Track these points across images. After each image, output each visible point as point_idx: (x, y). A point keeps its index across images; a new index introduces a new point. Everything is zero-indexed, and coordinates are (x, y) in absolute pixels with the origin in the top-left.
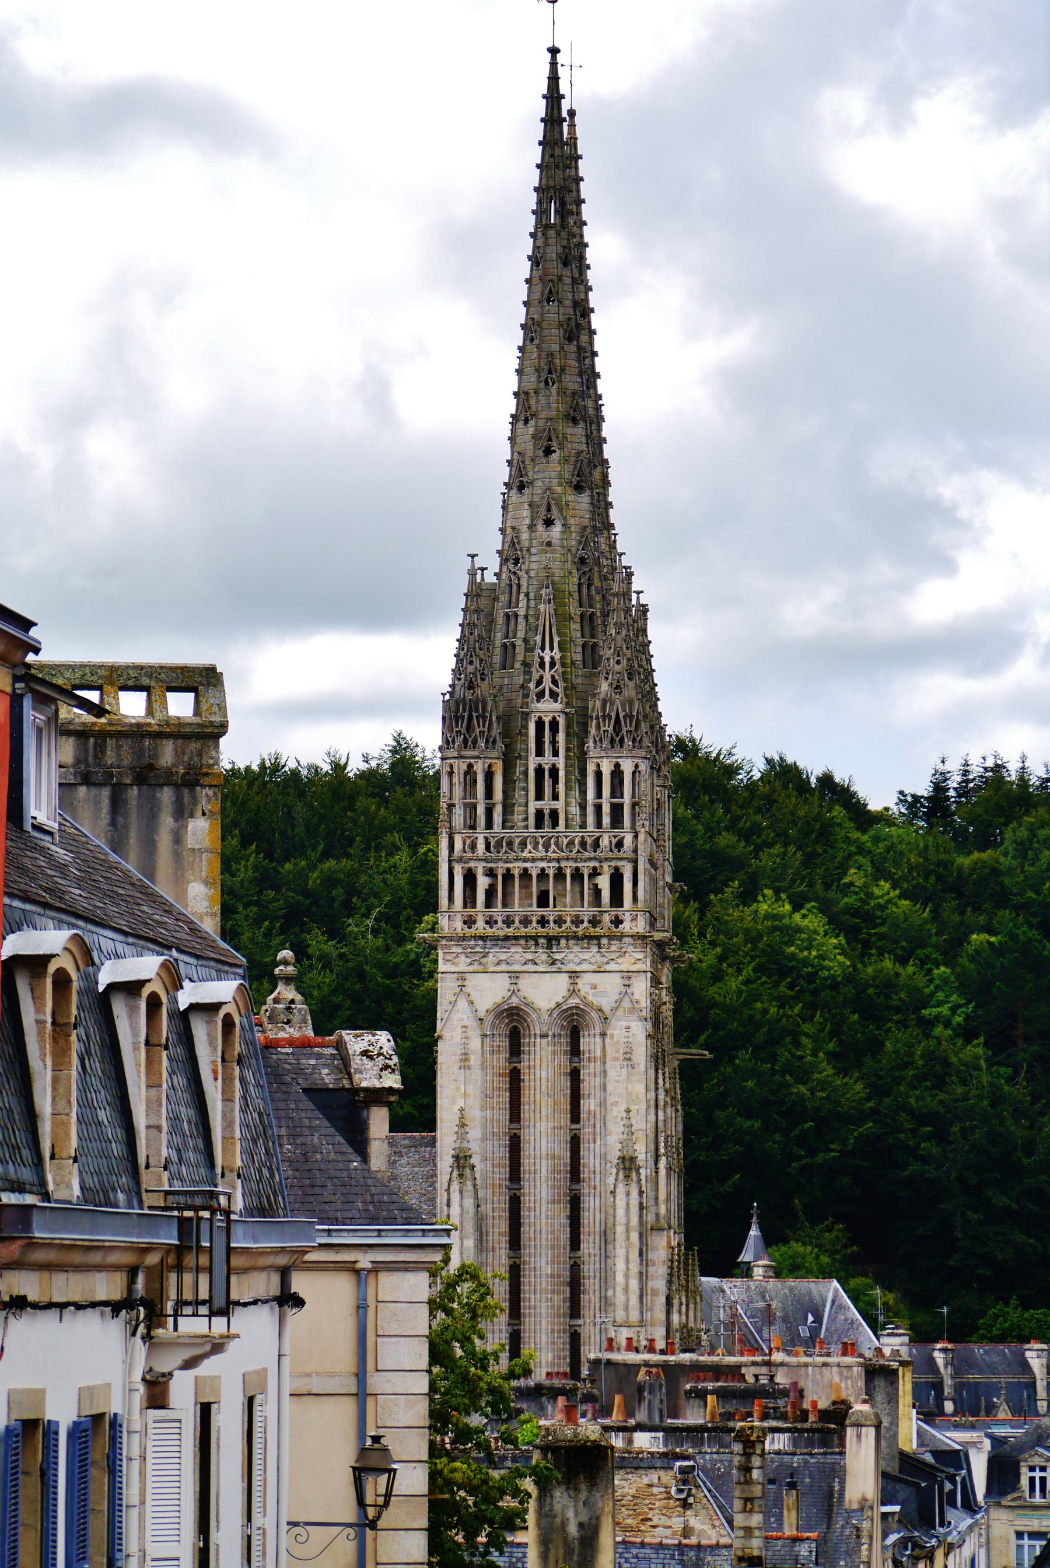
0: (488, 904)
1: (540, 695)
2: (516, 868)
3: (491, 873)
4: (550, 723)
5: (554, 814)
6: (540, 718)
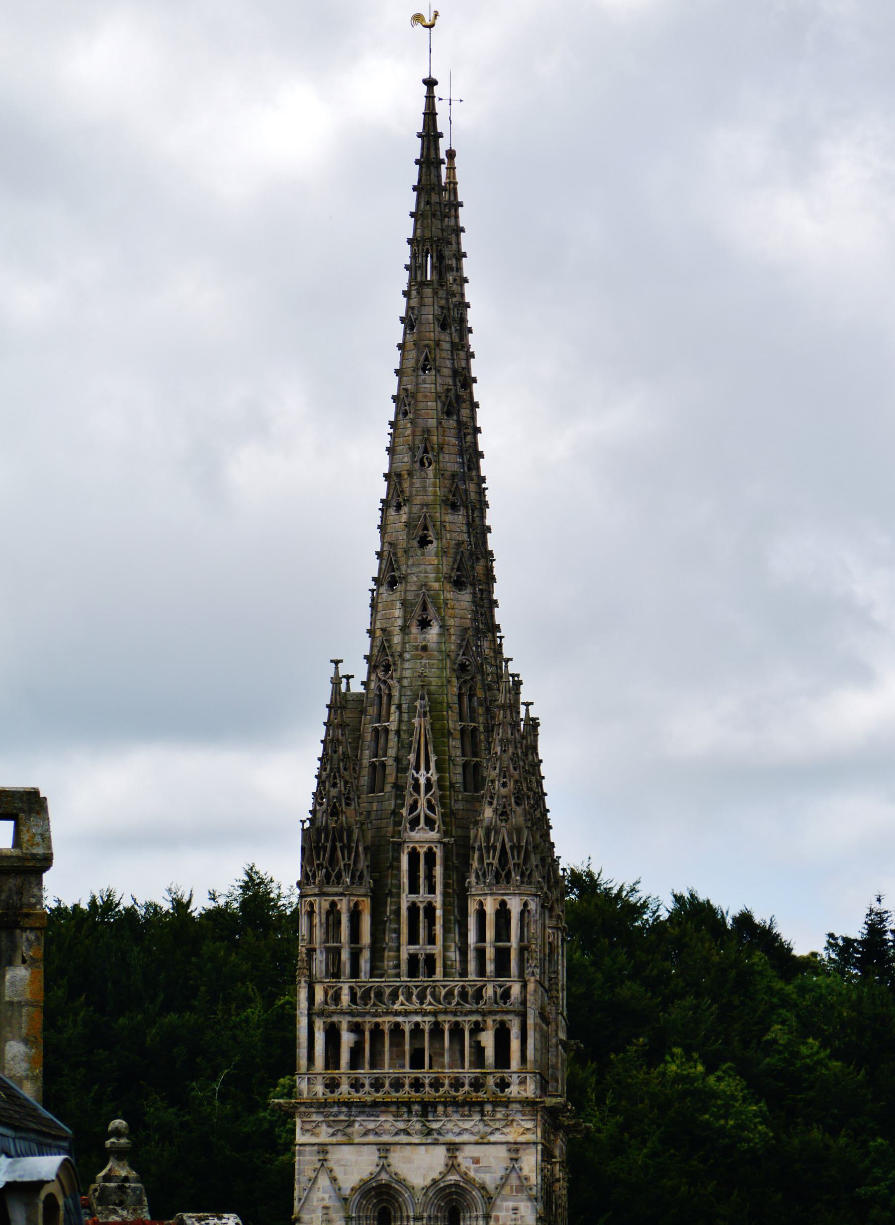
0: (355, 1063)
1: (414, 823)
2: (386, 1022)
3: (356, 1028)
4: (426, 854)
5: (430, 960)
6: (414, 849)
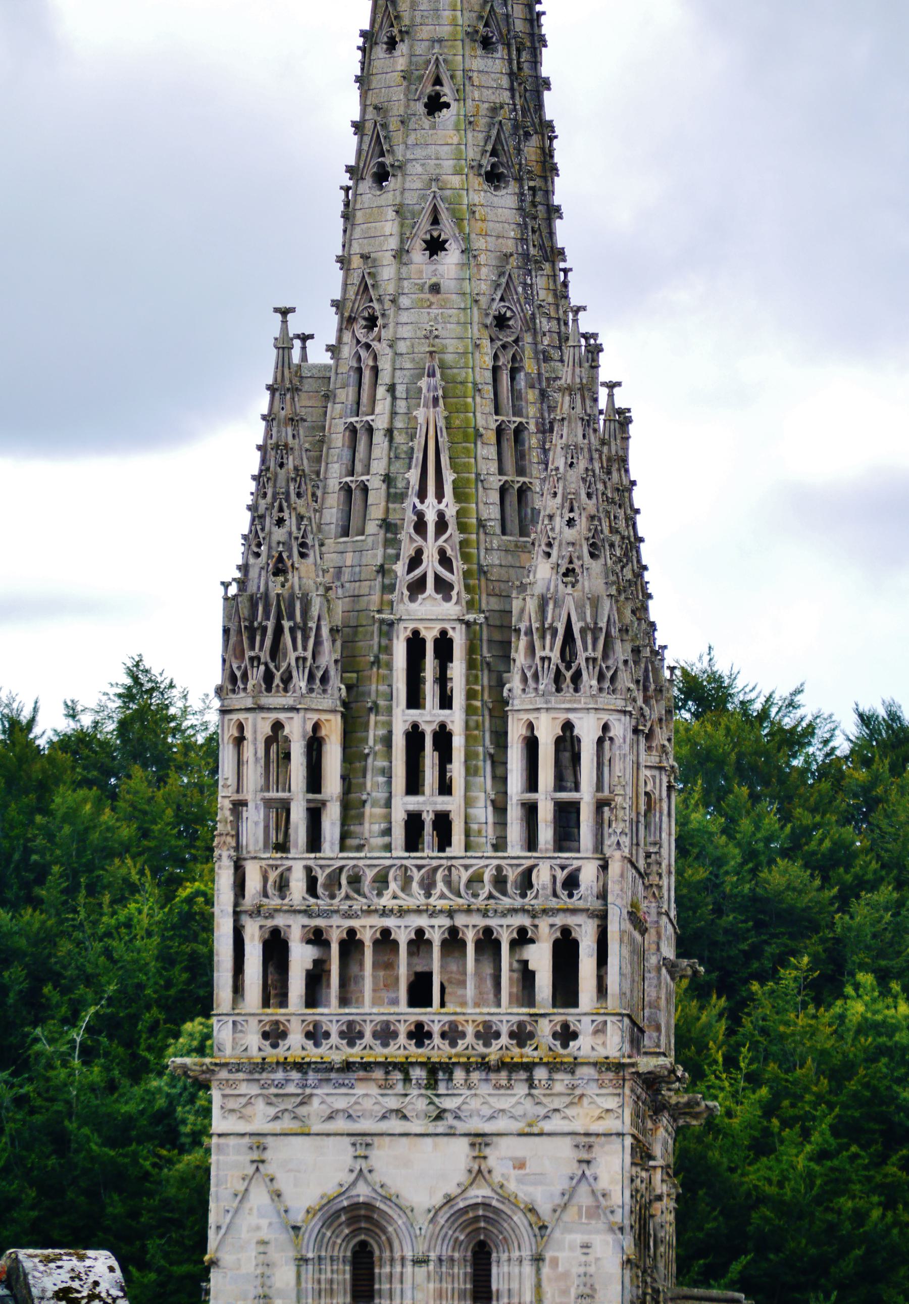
0: (312, 999)
1: (417, 587)
3: (317, 938)
4: (437, 642)
5: (443, 822)
6: (416, 633)
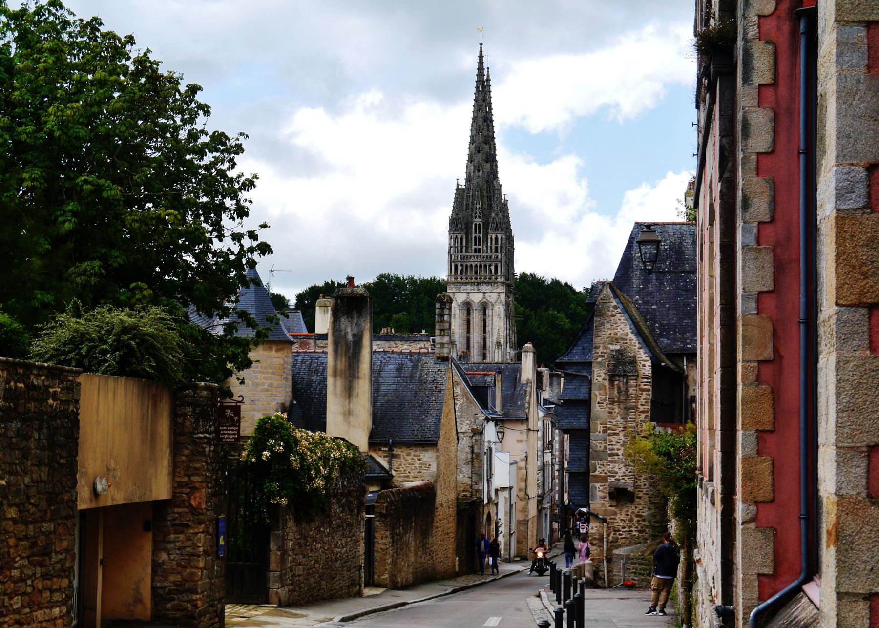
0: (462, 273)
1: (476, 217)
2: (469, 264)
3: (462, 265)
5: (479, 249)
